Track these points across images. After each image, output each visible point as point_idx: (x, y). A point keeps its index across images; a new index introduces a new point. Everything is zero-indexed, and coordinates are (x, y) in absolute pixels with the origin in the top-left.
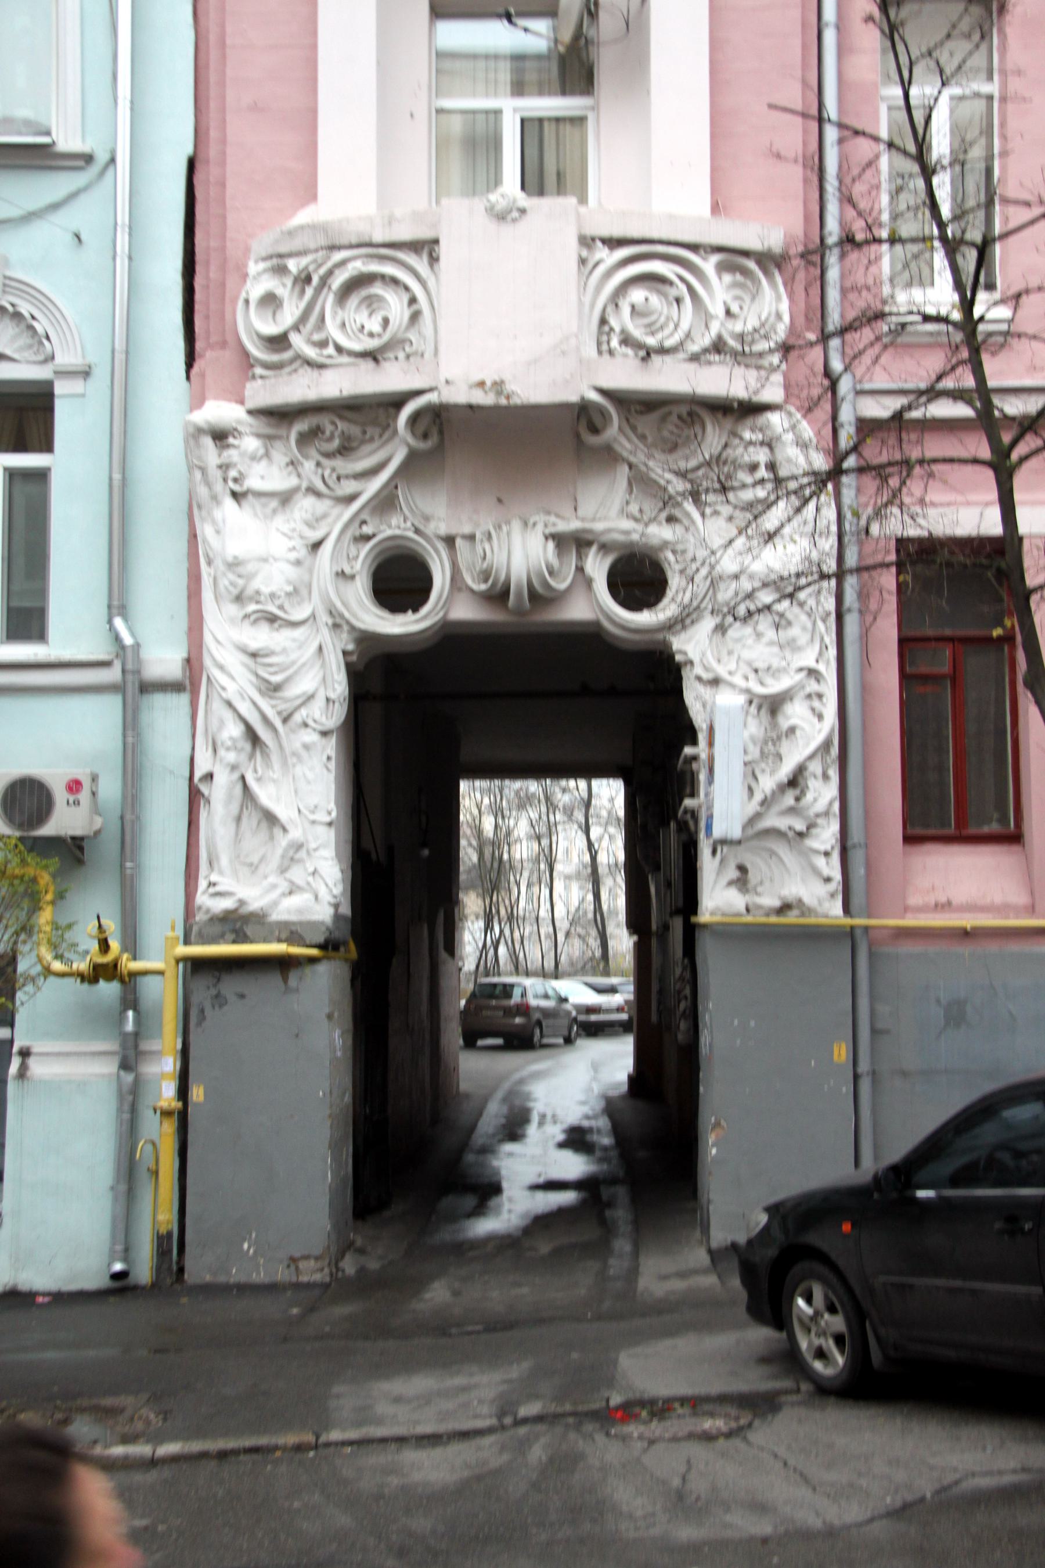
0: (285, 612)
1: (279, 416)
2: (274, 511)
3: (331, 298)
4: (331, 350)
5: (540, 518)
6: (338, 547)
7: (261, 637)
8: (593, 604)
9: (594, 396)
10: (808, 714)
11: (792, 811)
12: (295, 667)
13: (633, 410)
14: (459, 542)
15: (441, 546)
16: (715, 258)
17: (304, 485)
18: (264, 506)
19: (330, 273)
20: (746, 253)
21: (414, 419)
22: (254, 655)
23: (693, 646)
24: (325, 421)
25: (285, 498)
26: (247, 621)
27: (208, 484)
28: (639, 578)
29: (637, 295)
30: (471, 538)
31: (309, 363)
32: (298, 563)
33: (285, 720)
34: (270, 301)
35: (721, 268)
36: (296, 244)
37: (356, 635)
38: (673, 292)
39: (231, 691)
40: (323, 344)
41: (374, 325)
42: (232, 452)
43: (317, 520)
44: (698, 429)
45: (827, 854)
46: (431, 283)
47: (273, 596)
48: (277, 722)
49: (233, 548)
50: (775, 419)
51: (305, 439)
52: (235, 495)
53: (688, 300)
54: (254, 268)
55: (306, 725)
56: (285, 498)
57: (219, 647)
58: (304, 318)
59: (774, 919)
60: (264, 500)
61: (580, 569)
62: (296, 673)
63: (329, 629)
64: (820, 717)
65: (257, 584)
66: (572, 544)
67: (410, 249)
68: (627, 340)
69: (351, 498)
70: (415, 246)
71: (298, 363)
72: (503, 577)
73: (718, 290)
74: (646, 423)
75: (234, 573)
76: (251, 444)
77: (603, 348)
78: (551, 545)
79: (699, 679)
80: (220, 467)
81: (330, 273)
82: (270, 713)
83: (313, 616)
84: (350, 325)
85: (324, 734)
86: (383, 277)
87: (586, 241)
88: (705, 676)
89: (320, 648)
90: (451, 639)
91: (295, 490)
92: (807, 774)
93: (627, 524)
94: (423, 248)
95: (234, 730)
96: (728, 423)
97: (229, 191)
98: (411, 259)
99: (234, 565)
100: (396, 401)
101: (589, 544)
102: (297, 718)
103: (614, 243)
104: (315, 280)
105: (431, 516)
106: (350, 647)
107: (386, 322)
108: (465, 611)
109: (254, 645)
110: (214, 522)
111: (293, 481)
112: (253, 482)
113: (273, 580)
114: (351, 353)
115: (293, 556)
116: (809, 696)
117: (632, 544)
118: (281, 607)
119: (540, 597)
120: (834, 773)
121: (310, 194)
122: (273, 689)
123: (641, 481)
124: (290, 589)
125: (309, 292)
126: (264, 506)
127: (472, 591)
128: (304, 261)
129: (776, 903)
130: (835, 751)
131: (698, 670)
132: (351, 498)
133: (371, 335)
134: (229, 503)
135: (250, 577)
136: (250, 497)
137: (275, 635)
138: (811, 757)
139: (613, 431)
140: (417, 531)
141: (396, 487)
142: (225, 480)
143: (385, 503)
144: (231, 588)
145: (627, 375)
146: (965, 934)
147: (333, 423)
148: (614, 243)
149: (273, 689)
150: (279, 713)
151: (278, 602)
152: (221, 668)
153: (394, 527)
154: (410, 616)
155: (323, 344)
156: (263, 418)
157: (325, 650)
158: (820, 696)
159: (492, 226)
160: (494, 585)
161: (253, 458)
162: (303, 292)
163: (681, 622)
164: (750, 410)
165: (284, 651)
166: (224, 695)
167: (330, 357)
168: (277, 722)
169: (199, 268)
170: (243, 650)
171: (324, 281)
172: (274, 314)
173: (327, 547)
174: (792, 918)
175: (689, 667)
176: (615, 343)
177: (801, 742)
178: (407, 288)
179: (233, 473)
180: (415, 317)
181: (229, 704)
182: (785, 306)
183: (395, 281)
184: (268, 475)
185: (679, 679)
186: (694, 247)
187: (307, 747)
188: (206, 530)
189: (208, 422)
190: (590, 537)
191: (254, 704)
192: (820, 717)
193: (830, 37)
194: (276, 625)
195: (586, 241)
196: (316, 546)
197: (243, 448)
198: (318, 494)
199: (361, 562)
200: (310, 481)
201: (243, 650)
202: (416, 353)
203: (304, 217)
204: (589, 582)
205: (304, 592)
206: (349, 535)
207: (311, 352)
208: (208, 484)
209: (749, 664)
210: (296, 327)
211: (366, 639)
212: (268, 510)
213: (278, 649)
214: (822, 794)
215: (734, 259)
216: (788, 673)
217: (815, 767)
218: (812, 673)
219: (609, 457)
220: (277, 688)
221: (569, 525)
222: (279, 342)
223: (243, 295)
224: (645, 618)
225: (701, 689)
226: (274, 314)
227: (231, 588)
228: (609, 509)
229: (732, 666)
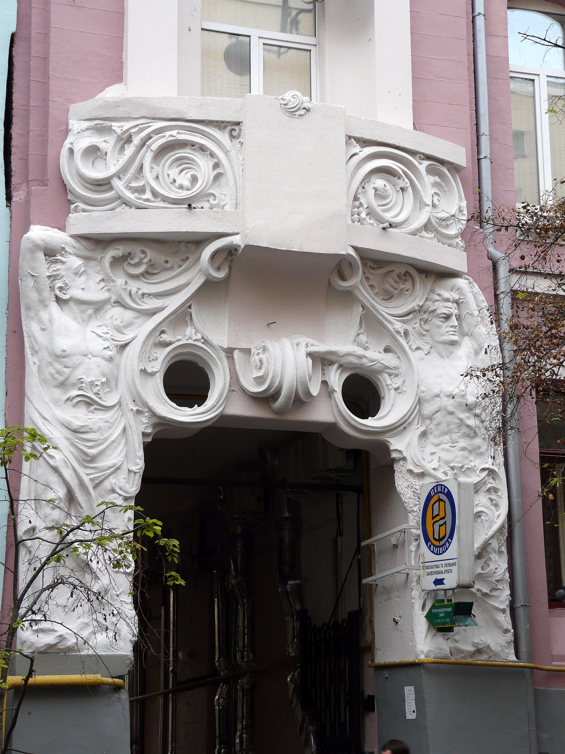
0: (100, 398)
1: (97, 242)
2: (90, 317)
3: (149, 156)
4: (148, 195)
5: (303, 340)
6: (144, 348)
7: (80, 417)
8: (329, 410)
9: (352, 252)
10: (488, 503)
12: (107, 444)
13: (368, 265)
14: (236, 354)
15: (223, 355)
16: (426, 163)
17: (114, 299)
18: (83, 312)
19: (149, 137)
20: (442, 162)
21: (214, 255)
22: (75, 431)
24: (136, 249)
25: (98, 307)
26: (69, 403)
27: (39, 290)
28: (363, 394)
29: (379, 182)
31: (127, 203)
32: (110, 359)
33: (95, 487)
34: (93, 152)
35: (430, 171)
36: (120, 112)
37: (155, 420)
39: (57, 458)
40: (141, 190)
41: (184, 179)
42: (59, 266)
43: (125, 327)
44: (408, 285)
47: (92, 384)
48: (90, 486)
49: (63, 343)
50: (461, 282)
51: (117, 262)
52: (58, 300)
54: (75, 125)
56: (98, 307)
57: (45, 422)
58: (125, 169)
59: (469, 660)
60: (83, 307)
62: (107, 447)
63: (134, 416)
64: (496, 506)
65: (79, 374)
66: (322, 361)
67: (215, 126)
68: (371, 213)
69: (152, 313)
70: (220, 125)
71: (118, 202)
72: (276, 384)
73: (427, 184)
75: (61, 363)
76: (75, 262)
78: (310, 361)
79: (410, 471)
80: (49, 277)
81: (149, 137)
82: (86, 479)
83: (119, 403)
84: (170, 179)
86: (193, 145)
88: (416, 471)
89: (124, 430)
90: (221, 431)
91: (106, 302)
92: (489, 549)
94: (226, 127)
95: (61, 492)
96: (429, 283)
97: (52, 65)
99: (60, 357)
100: (198, 241)
101: (332, 363)
102: (107, 485)
103: (365, 143)
104: (136, 140)
105: (213, 333)
106: (149, 430)
107: (194, 179)
108: (240, 409)
109: (76, 423)
110: (40, 321)
111: (104, 295)
112: (75, 292)
113: (91, 371)
114: (165, 199)
116: (489, 490)
117: (361, 367)
118: (97, 394)
119: (300, 400)
120: (504, 549)
121: (117, 75)
122: (88, 460)
124: (104, 380)
125: (130, 150)
126: (83, 312)
127: (244, 391)
128: (127, 125)
129: (472, 649)
130: (506, 531)
132: (152, 313)
133: (181, 187)
134: (54, 306)
135: (75, 367)
136: (72, 304)
137: (90, 416)
138: (492, 537)
141: (190, 307)
142: (52, 288)
143: (182, 316)
144: (57, 376)
147: (143, 252)
148: (365, 143)
149: (88, 460)
150: (92, 480)
151: (95, 390)
153: (186, 336)
154: (197, 409)
155: (141, 190)
156: (84, 243)
157: (129, 432)
158: (496, 490)
159: (285, 118)
160: (269, 388)
161: (77, 273)
162: (122, 149)
163: (399, 428)
164: (444, 274)
165: (100, 429)
166: (51, 462)
167: (148, 200)
168: (90, 486)
169: (15, 120)
170: (67, 426)
171: (143, 143)
172: (93, 162)
173: (133, 350)
174: (482, 659)
175: (401, 463)
176: (363, 215)
177: (486, 524)
178: (212, 155)
179: (59, 284)
180: (217, 177)
181: (56, 470)
182: (464, 204)
183: (202, 149)
184: (88, 286)
185: (392, 472)
186: (413, 153)
188: (31, 327)
189: (43, 240)
190: (333, 358)
191: (75, 471)
192: (496, 506)
193: (480, 22)
194: (92, 408)
196: (124, 347)
197: (68, 264)
198: (125, 307)
199: (159, 362)
200: (120, 296)
201: (67, 426)
202: (217, 206)
203: (112, 93)
205: (113, 383)
206: (151, 341)
207: (130, 196)
208: (39, 290)
209: (447, 463)
211: (163, 425)
212: (85, 316)
213: (95, 428)
214: (499, 565)
215: (437, 163)
216: (475, 471)
217: (495, 544)
218: (491, 472)
219: (348, 297)
220: (93, 459)
221: (321, 348)
222: (103, 185)
223: (67, 145)
224: (371, 422)
226: (93, 162)
227: (57, 376)
228: (345, 340)
229: (435, 464)
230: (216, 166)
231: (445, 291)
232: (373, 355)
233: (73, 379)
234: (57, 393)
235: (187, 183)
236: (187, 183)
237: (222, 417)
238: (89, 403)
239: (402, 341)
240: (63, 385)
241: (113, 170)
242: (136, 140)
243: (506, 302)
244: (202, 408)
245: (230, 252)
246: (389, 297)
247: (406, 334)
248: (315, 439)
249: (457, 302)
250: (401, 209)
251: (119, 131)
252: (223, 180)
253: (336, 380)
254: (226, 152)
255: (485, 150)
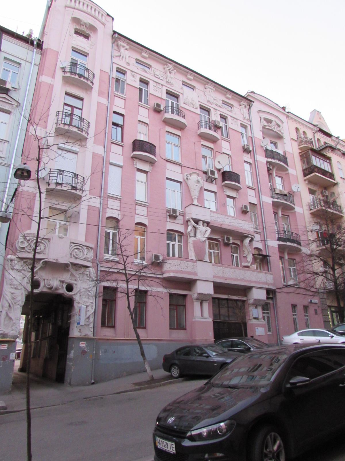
1: (22, 259)
7: (13, 291)
8: (63, 291)
9: (69, 263)
11: (87, 322)
14: (46, 280)
15: (43, 280)
19: (33, 240)
22: (12, 293)
23: (77, 298)
29: (76, 250)
30: (48, 279)
38: (80, 251)
39: (8, 298)
45: (92, 328)
46: (48, 245)
48: (14, 304)
53: (82, 252)
55: (18, 305)
61: (62, 286)
66: (63, 282)
68: (74, 256)
70: (47, 239)
74: (74, 267)
77: (71, 257)
79: (77, 302)
81: (33, 240)
82: (13, 302)
85: (21, 306)
87: (71, 243)
90: (41, 294)
93: (69, 280)
95: (8, 305)
98: (46, 241)
101: (64, 282)
102: (17, 303)
103: (74, 243)
104: (31, 241)
107: (41, 248)
108: (45, 290)
109: (12, 292)
115: (20, 279)
117: (70, 283)
119: (57, 289)
123: (72, 275)
127: (46, 287)
131: (77, 301)
139: (70, 268)
140: (40, 278)
145: (73, 261)
146: (108, 339)
148: (74, 243)
152: (7, 295)
171: (32, 241)
178: (45, 244)
181: (7, 301)
183: (43, 243)
187: (18, 308)
195: (71, 243)
204: (63, 288)
207: (29, 251)
210: (26, 247)
220: (15, 299)
224: (70, 293)
225: (77, 304)
230: (45, 246)
231: (87, 270)
232: (72, 282)
233: (13, 283)
234: (10, 286)
235: (39, 249)
236: (39, 249)
237: (42, 291)
238: (15, 288)
239: (78, 279)
240: (11, 285)
241: (26, 246)
242: (31, 241)
243: (99, 272)
244: (38, 290)
245: (46, 262)
246: (76, 270)
247: (79, 277)
248: (60, 296)
249: (89, 272)
250: (80, 255)
251: (28, 239)
252: (46, 249)
253: (65, 285)
254: (47, 244)
255: (99, 245)
